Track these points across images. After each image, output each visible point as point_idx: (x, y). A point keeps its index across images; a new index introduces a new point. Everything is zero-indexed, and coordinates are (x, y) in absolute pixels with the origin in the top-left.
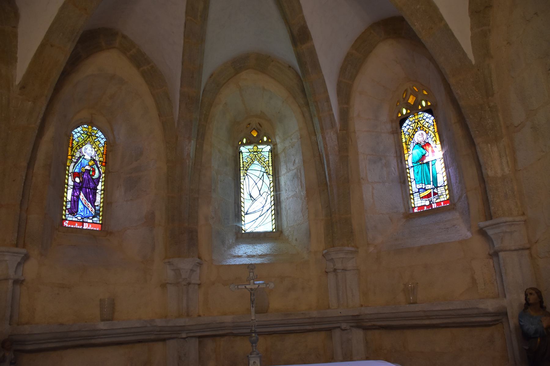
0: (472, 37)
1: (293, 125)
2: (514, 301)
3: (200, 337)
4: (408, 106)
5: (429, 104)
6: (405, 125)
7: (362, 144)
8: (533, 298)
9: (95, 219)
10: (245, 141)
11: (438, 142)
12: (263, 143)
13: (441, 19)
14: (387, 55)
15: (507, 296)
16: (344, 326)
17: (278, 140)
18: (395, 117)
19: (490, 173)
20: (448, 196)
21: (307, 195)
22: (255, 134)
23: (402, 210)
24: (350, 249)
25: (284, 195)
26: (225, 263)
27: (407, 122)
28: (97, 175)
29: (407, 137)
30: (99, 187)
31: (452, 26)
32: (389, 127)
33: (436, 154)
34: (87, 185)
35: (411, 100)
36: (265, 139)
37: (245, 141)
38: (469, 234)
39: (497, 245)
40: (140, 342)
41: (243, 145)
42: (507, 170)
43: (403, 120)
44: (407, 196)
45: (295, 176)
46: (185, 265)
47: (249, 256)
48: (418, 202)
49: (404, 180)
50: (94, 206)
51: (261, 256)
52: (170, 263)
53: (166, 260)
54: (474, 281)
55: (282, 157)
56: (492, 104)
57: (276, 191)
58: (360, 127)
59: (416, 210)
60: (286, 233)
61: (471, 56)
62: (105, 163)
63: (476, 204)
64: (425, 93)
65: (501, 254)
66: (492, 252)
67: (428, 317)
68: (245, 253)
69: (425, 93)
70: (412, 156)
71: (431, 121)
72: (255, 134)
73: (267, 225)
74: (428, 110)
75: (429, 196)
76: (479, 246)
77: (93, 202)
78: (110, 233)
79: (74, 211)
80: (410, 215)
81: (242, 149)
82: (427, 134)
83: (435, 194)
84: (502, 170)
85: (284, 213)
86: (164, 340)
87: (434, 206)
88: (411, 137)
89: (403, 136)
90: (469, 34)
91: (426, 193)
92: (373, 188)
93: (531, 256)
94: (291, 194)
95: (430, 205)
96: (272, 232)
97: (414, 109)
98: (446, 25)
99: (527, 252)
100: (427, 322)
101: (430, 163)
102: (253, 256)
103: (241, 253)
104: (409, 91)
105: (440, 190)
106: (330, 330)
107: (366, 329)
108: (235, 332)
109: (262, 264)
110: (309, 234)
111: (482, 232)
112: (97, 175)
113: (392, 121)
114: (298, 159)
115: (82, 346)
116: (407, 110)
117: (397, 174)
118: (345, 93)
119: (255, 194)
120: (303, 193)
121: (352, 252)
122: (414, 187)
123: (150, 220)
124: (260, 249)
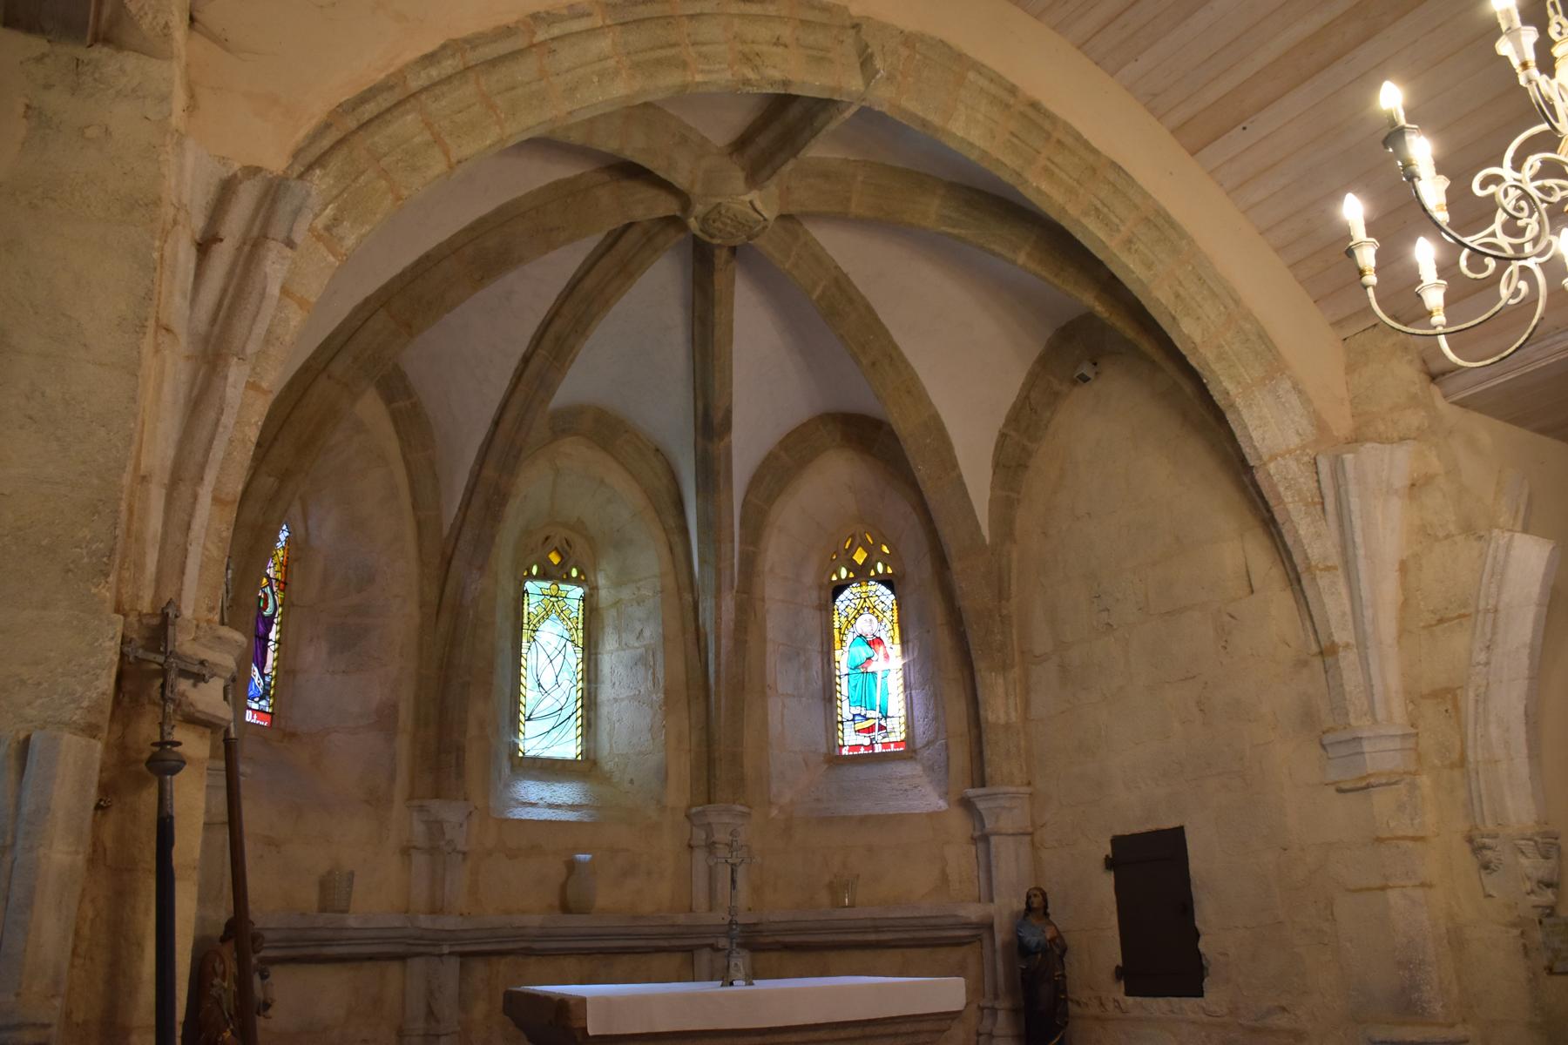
0: (991, 501)
1: (650, 560)
2: (1007, 905)
3: (462, 955)
4: (852, 566)
5: (890, 571)
6: (841, 597)
7: (775, 623)
8: (1036, 902)
9: (263, 703)
10: (535, 570)
11: (897, 640)
12: (568, 580)
13: (955, 466)
14: (836, 477)
15: (996, 900)
16: (723, 942)
17: (602, 581)
18: (826, 581)
19: (991, 717)
20: (903, 736)
21: (666, 702)
22: (555, 559)
23: (823, 749)
24: (739, 808)
25: (606, 692)
26: (510, 816)
27: (846, 593)
28: (268, 612)
29: (843, 619)
30: (273, 635)
31: (967, 479)
32: (813, 597)
33: (891, 664)
35: (860, 557)
36: (574, 573)
37: (535, 570)
38: (942, 805)
39: (989, 825)
40: (371, 958)
41: (531, 577)
42: (1014, 717)
43: (839, 589)
44: (832, 724)
45: (641, 661)
46: (450, 813)
47: (550, 806)
48: (850, 738)
49: (829, 696)
50: (263, 675)
51: (572, 807)
52: (421, 808)
53: (416, 802)
54: (944, 877)
55: (609, 617)
56: (1004, 612)
57: (589, 682)
58: (773, 591)
59: (845, 751)
61: (985, 531)
63: (960, 759)
64: (885, 549)
65: (994, 840)
66: (977, 834)
68: (542, 800)
69: (885, 549)
71: (888, 602)
72: (555, 559)
73: (567, 747)
74: (887, 582)
75: (870, 729)
76: (958, 824)
78: (292, 736)
80: (835, 760)
81: (529, 585)
82: (880, 622)
83: (881, 728)
84: (1007, 714)
85: (604, 727)
87: (878, 749)
88: (851, 622)
89: (836, 617)
90: (987, 495)
91: (867, 724)
92: (784, 706)
93: (1033, 844)
94: (625, 693)
95: (872, 746)
96: (575, 761)
97: (862, 574)
98: (960, 476)
99: (1028, 838)
100: (872, 937)
101: (879, 676)
102: (558, 806)
103: (533, 798)
104: (858, 540)
105: (890, 724)
106: (690, 950)
108: (537, 946)
109: (579, 824)
110: (663, 775)
111: (967, 804)
112: (268, 612)
113: (820, 587)
114: (651, 632)
116: (849, 571)
117: (820, 683)
119: (548, 681)
121: (743, 815)
122: (846, 710)
123: (385, 719)
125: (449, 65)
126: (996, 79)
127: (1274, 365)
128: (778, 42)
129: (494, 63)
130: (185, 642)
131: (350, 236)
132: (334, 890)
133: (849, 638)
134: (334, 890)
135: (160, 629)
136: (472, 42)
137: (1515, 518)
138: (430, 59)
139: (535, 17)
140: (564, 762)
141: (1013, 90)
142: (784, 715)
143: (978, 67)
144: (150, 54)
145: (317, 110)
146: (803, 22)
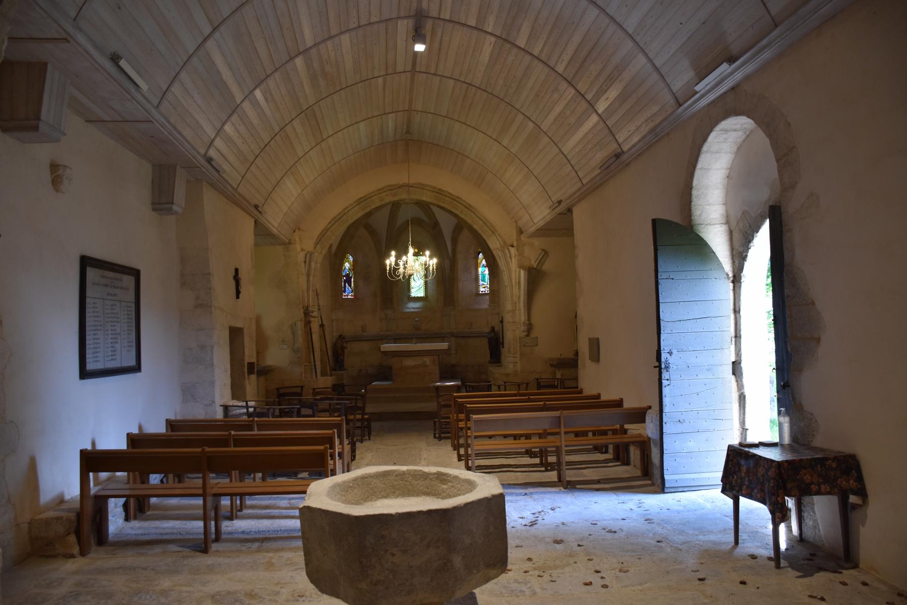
23: (475, 292)
34: (348, 281)
44: (478, 286)
48: (482, 289)
62: (353, 269)
70: (480, 270)
73: (421, 294)
77: (350, 285)
79: (345, 291)
80: (478, 294)
118: (454, 241)
122: (481, 283)
124: (418, 305)
127: (494, 231)
130: (311, 309)
131: (324, 252)
135: (307, 307)
141: (435, 188)
142: (464, 285)
143: (427, 186)
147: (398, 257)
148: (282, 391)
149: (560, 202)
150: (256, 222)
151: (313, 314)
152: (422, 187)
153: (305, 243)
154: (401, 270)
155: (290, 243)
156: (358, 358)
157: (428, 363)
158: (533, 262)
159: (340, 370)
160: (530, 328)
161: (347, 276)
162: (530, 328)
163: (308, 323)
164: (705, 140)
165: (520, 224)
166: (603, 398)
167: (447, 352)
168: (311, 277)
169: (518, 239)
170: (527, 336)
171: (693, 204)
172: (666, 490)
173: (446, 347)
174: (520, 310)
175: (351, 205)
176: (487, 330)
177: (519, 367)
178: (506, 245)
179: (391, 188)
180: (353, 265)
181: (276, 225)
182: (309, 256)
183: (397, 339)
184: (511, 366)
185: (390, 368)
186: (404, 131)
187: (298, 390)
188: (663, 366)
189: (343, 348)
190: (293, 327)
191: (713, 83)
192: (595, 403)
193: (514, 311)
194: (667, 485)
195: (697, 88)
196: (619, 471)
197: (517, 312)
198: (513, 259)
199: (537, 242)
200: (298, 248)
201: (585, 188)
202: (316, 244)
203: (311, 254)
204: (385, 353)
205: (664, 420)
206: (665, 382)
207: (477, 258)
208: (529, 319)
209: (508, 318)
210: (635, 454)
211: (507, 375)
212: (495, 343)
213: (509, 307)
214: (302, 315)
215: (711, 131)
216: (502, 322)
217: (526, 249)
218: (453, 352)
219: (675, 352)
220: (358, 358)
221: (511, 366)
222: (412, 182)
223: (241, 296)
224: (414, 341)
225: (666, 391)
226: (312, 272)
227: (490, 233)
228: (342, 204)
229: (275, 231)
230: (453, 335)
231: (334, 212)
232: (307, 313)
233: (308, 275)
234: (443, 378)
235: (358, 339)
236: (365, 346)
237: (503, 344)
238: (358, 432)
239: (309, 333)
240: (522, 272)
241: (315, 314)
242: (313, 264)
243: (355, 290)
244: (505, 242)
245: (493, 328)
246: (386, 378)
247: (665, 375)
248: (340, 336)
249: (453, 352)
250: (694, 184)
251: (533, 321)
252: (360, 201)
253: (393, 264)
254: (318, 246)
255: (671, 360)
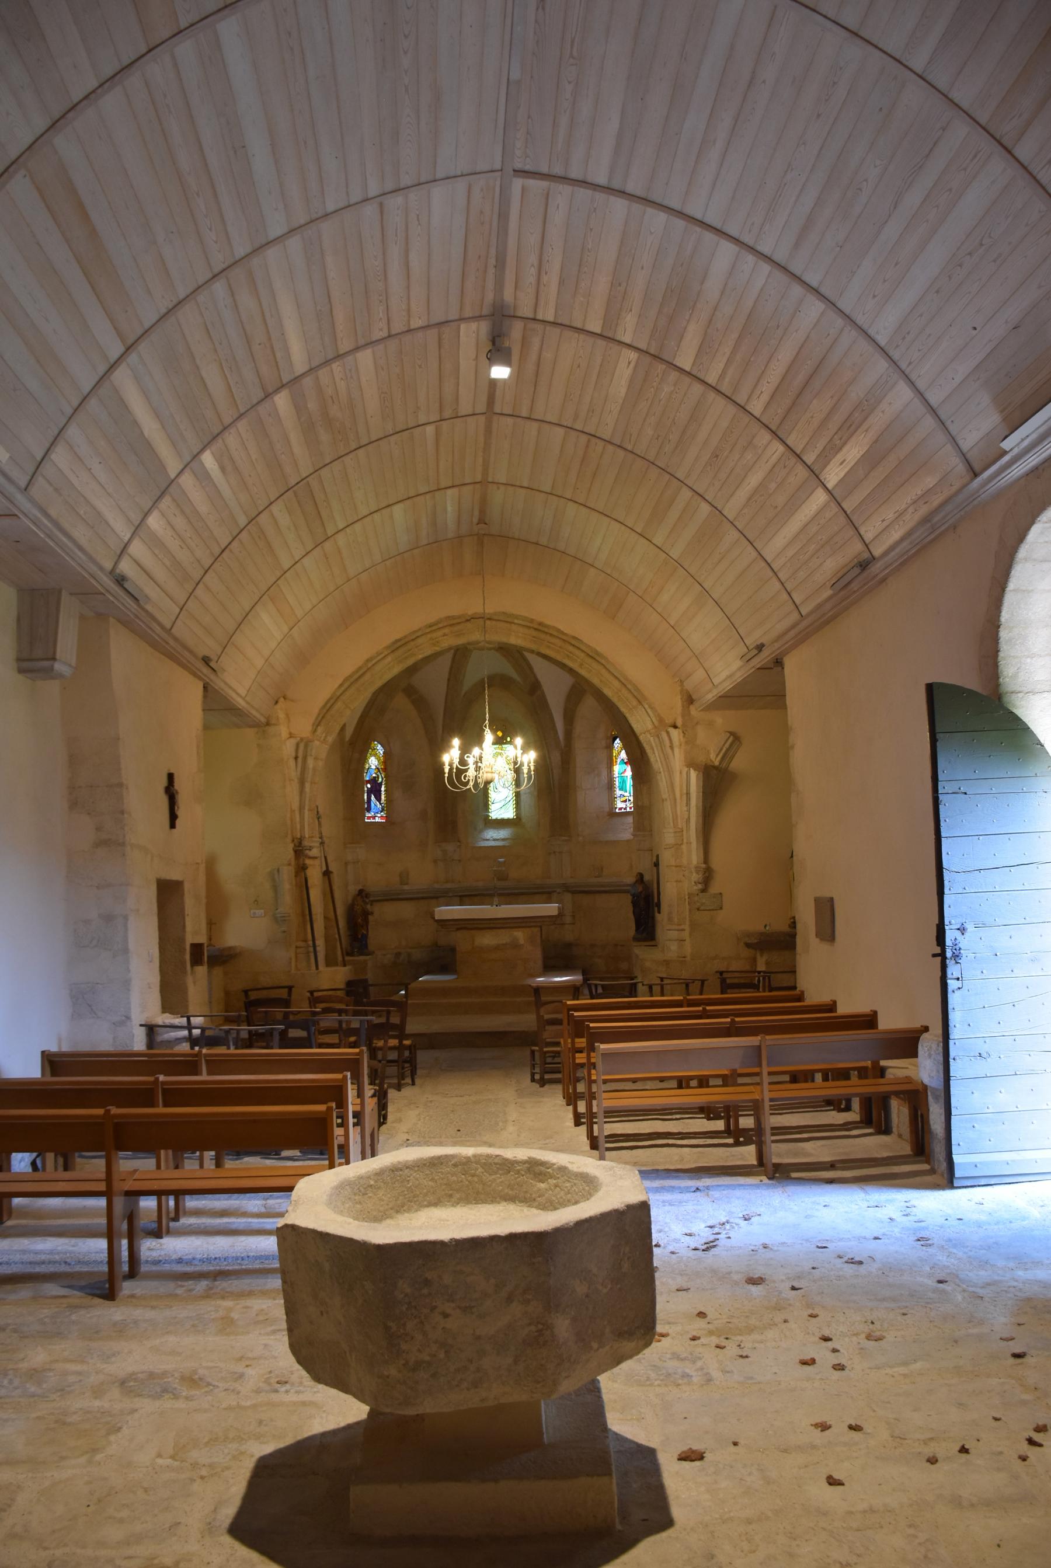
23: (607, 810)
30: (383, 789)
32: (604, 743)
34: (375, 790)
40: (423, 898)
44: (612, 799)
46: (450, 847)
48: (620, 804)
51: (503, 840)
60: (524, 820)
62: (385, 770)
67: (602, 886)
68: (493, 837)
70: (617, 769)
73: (509, 813)
75: (625, 801)
77: (379, 799)
79: (369, 810)
80: (613, 814)
85: (522, 804)
86: (437, 898)
88: (619, 754)
106: (550, 893)
107: (573, 893)
109: (504, 847)
115: (392, 900)
120: (536, 793)
122: (618, 793)
124: (503, 833)
125: (346, 685)
126: (525, 619)
128: (445, 635)
129: (357, 680)
130: (306, 843)
131: (330, 739)
132: (404, 878)
133: (619, 761)
134: (404, 878)
135: (300, 841)
136: (350, 676)
137: (717, 755)
138: (341, 685)
139: (368, 661)
140: (508, 820)
141: (532, 621)
142: (586, 798)
143: (517, 617)
144: (274, 725)
145: (316, 711)
146: (451, 625)
147: (465, 750)
148: (253, 996)
149: (760, 648)
150: (205, 688)
151: (311, 853)
152: (508, 619)
153: (297, 723)
154: (471, 773)
155: (268, 724)
156: (393, 932)
157: (522, 942)
158: (712, 756)
159: (362, 954)
160: (707, 876)
161: (373, 781)
162: (707, 876)
163: (301, 869)
164: (1021, 538)
165: (689, 685)
166: (842, 1010)
167: (555, 920)
168: (307, 786)
169: (686, 713)
170: (703, 891)
171: (1001, 654)
172: (956, 1183)
173: (555, 913)
174: (689, 843)
175: (378, 654)
176: (630, 879)
177: (688, 949)
178: (664, 725)
179: (453, 622)
180: (385, 762)
181: (243, 692)
182: (303, 748)
183: (466, 897)
184: (674, 947)
185: (453, 950)
186: (475, 520)
187: (283, 994)
188: (949, 954)
189: (366, 914)
190: (274, 877)
191: (1034, 436)
192: (827, 1019)
193: (678, 846)
194: (958, 1173)
195: (1006, 445)
196: (870, 1144)
197: (684, 847)
198: (676, 750)
199: (719, 719)
200: (284, 732)
201: (805, 623)
202: (317, 724)
203: (307, 743)
204: (443, 923)
205: (952, 1054)
206: (952, 984)
207: (610, 747)
208: (706, 860)
209: (667, 858)
210: (899, 1113)
211: (667, 963)
212: (645, 904)
213: (669, 837)
214: (291, 854)
215: (1033, 523)
216: (656, 865)
217: (701, 733)
218: (568, 919)
219: (970, 927)
220: (393, 932)
221: (674, 947)
222: (490, 610)
223: (178, 822)
224: (496, 899)
225: (954, 999)
226: (309, 776)
227: (635, 703)
228: (363, 652)
229: (241, 703)
230: (567, 888)
231: (348, 668)
232: (299, 851)
233: (302, 782)
234: (551, 966)
235: (391, 897)
236: (406, 910)
237: (658, 905)
238: (392, 1070)
239: (304, 886)
240: (693, 774)
241: (315, 852)
242: (310, 762)
243: (389, 808)
244: (661, 720)
245: (641, 877)
246: (444, 969)
247: (953, 970)
248: (361, 892)
249: (568, 919)
250: (1003, 619)
251: (716, 862)
252: (397, 646)
253: (456, 762)
254: (320, 729)
255: (964, 942)
